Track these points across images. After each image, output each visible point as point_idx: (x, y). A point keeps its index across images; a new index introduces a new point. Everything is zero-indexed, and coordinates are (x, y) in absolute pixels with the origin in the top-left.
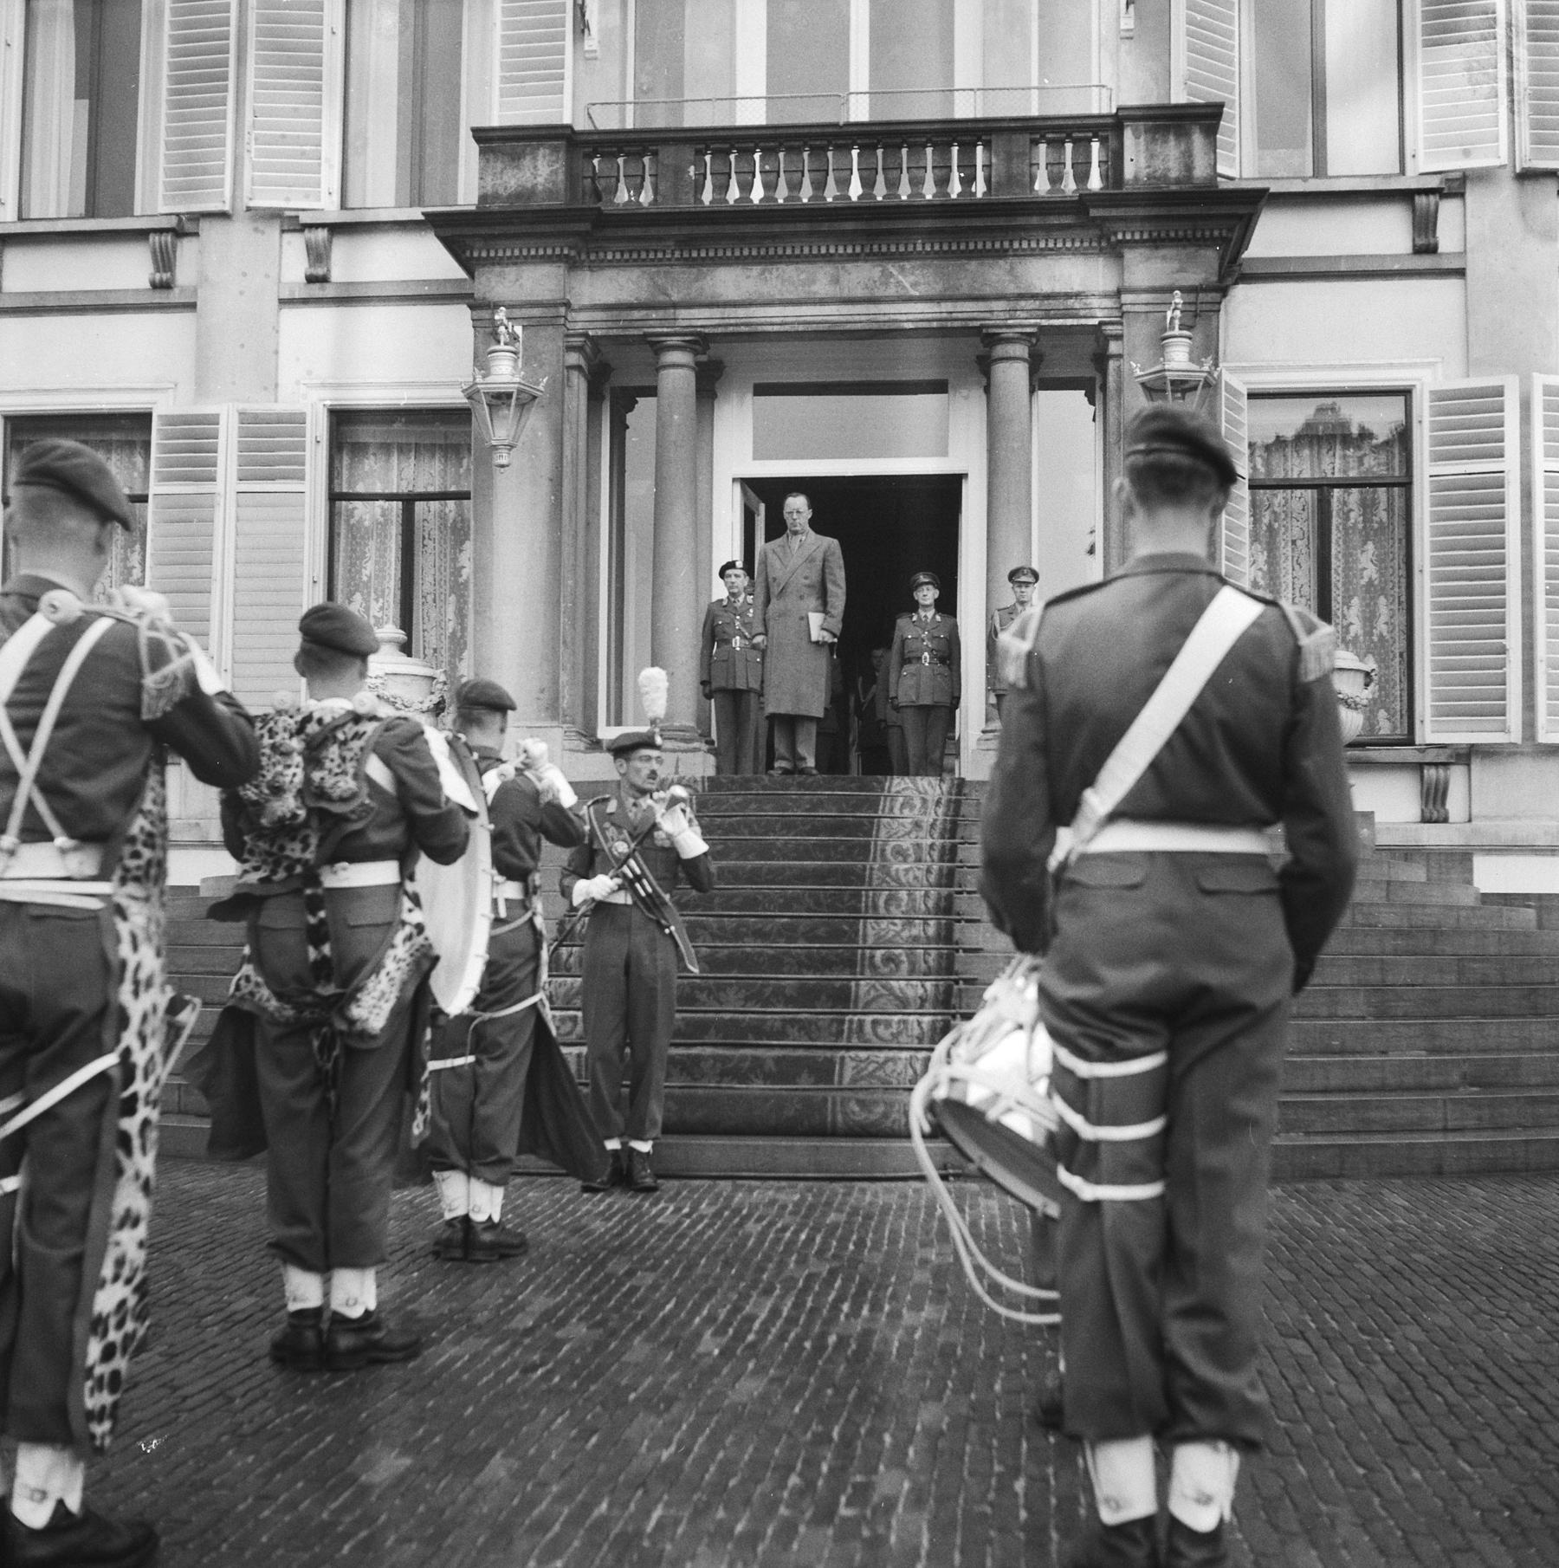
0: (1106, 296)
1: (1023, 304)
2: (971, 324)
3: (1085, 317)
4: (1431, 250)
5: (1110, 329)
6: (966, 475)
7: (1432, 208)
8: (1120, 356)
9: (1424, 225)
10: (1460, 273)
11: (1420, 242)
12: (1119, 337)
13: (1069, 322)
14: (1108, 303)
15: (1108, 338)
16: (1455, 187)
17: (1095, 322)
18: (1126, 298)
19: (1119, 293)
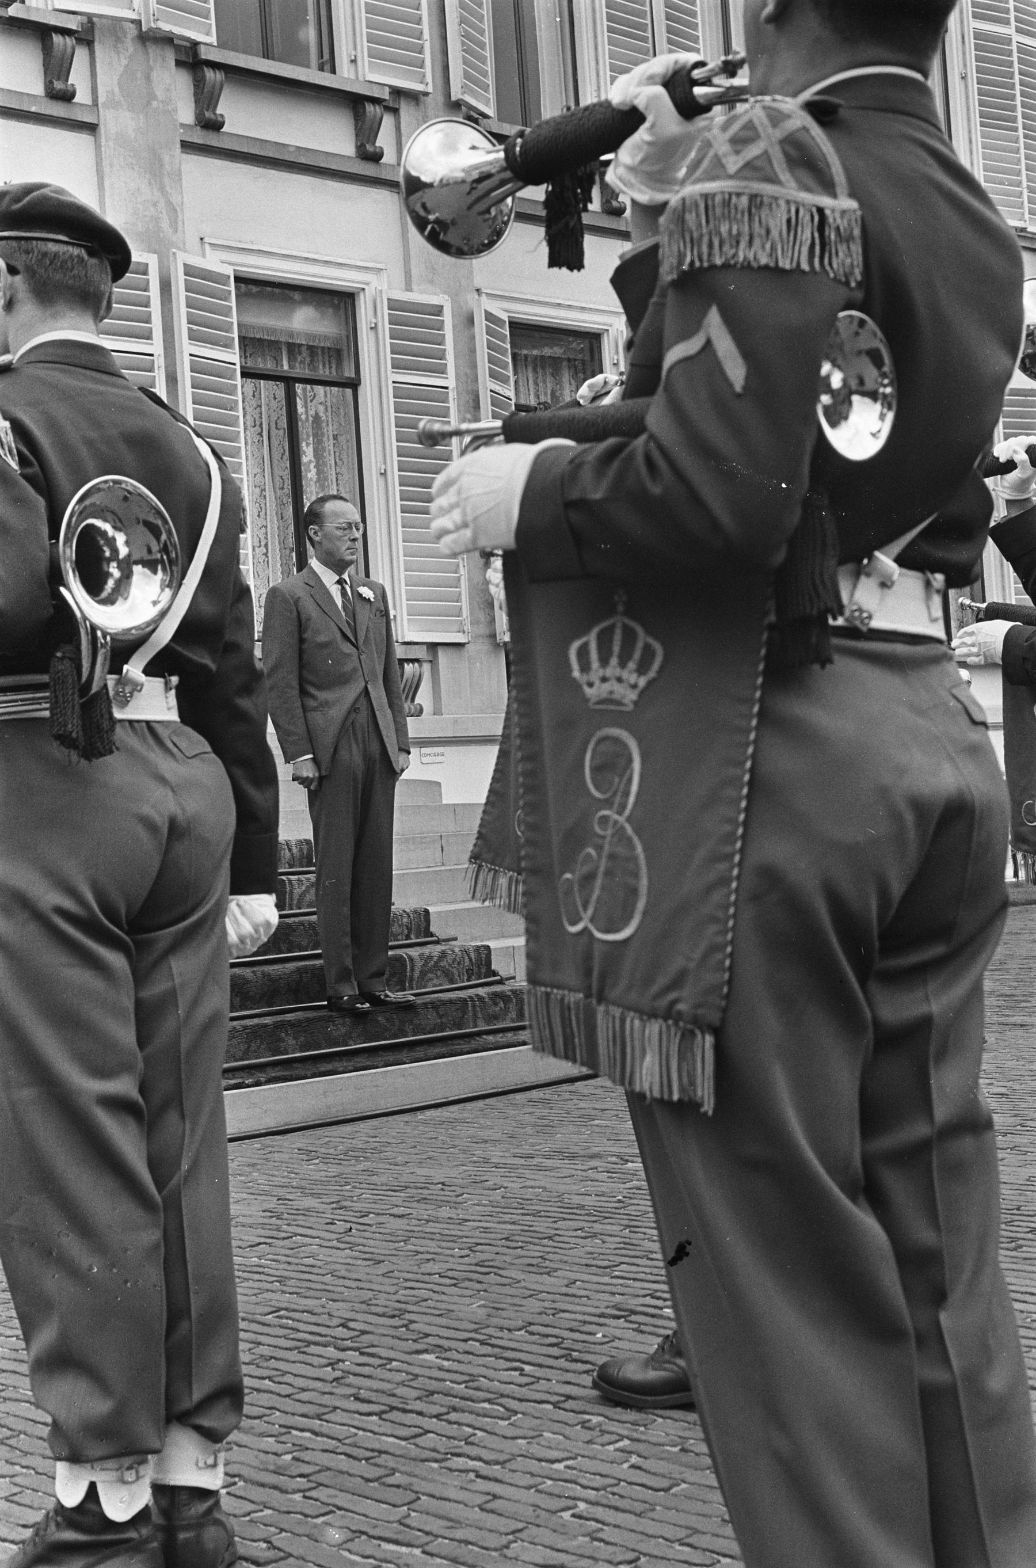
4: (67, 97)
7: (69, 50)
9: (56, 69)
10: (91, 128)
11: (58, 85)
16: (87, 33)
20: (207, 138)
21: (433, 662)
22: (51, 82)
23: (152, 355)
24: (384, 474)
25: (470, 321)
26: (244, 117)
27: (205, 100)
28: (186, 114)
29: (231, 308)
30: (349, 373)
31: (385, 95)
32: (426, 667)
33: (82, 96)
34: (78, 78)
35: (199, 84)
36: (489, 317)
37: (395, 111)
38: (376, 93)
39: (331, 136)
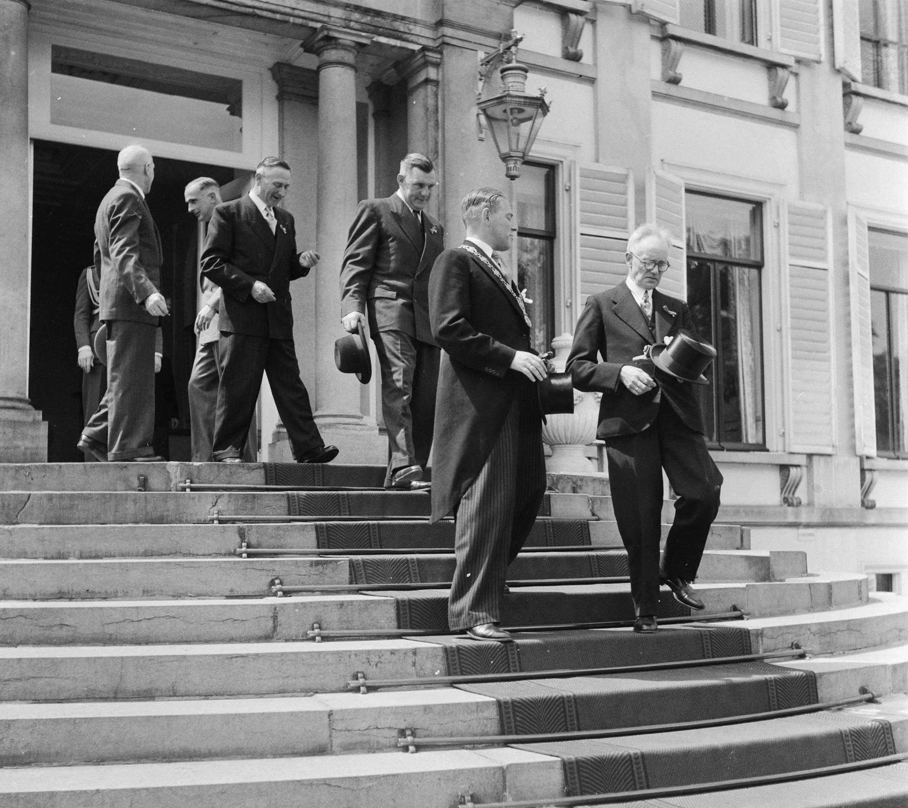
0: (425, 25)
1: (356, 16)
2: (311, 24)
4: (575, 58)
5: (433, 56)
8: (436, 83)
9: (571, 37)
10: (592, 81)
11: (572, 50)
12: (437, 65)
14: (428, 33)
15: (426, 64)
17: (417, 48)
18: (448, 31)
19: (441, 23)
21: (809, 466)
22: (567, 48)
23: (626, 240)
24: (780, 330)
25: (845, 222)
27: (670, 62)
28: (656, 71)
29: (681, 209)
30: (754, 257)
31: (791, 62)
32: (805, 470)
33: (587, 59)
34: (585, 46)
35: (666, 52)
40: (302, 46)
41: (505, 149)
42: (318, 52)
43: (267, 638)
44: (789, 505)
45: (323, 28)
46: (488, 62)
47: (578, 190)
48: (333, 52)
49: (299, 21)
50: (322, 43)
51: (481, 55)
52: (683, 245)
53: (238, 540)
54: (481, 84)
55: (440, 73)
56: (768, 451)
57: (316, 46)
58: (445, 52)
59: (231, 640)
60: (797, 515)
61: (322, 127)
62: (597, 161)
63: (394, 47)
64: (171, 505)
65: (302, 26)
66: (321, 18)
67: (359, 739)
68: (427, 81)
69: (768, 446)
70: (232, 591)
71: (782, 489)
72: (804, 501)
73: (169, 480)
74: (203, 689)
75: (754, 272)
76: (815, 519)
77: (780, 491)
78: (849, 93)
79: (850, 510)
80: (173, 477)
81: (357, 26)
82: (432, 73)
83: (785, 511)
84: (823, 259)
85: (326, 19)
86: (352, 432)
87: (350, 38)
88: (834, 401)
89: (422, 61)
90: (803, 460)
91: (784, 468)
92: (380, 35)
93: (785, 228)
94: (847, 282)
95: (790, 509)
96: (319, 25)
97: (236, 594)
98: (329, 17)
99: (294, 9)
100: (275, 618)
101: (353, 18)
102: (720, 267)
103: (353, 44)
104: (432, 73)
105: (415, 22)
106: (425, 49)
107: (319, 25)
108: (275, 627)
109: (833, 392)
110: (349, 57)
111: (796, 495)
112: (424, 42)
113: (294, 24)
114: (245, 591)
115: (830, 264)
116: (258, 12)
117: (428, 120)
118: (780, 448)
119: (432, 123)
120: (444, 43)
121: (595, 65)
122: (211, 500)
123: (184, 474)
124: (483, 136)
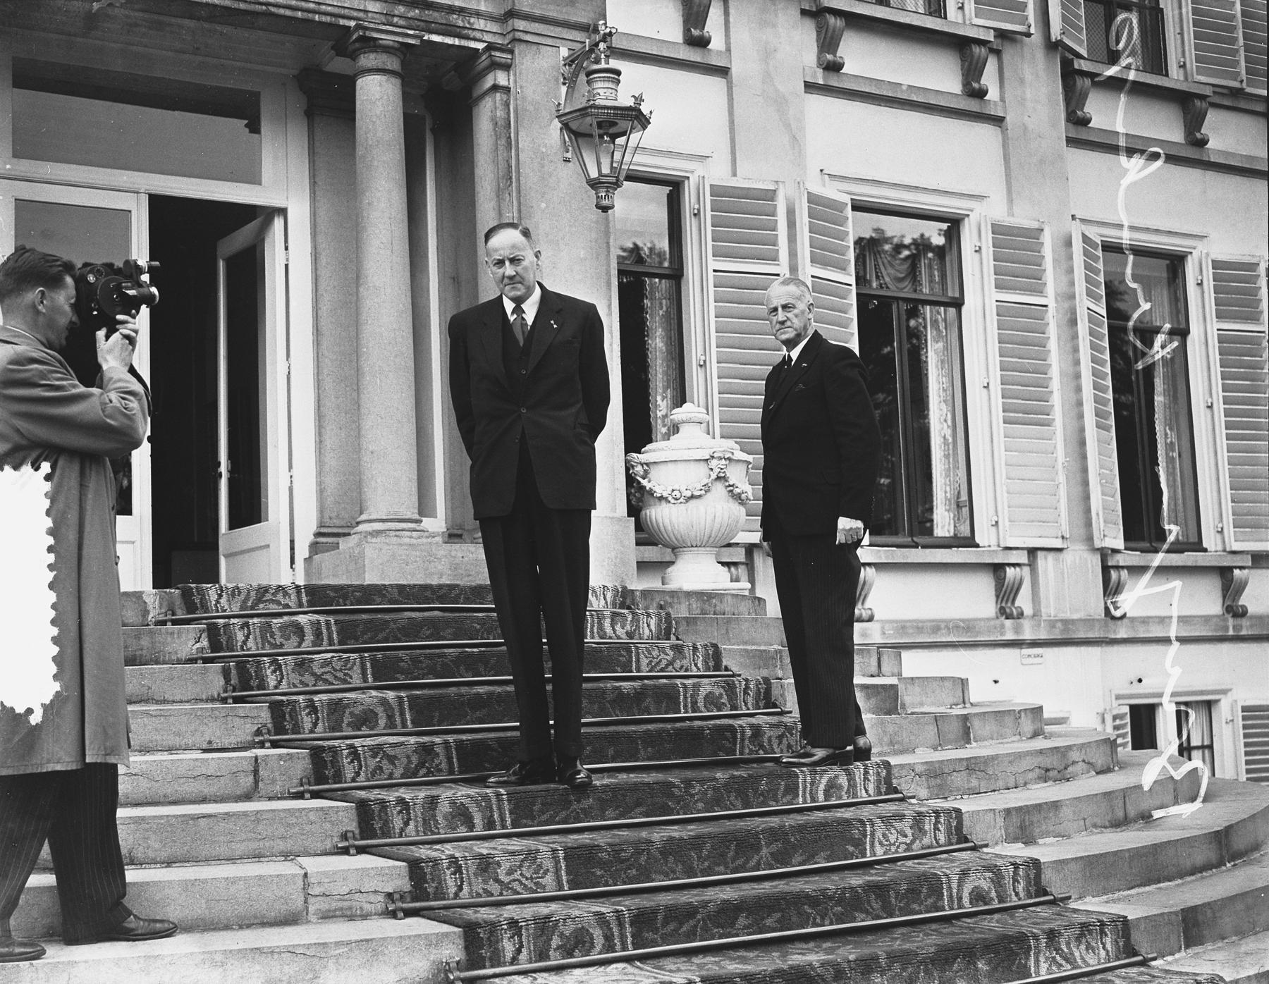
2: (342, 22)
3: (468, 38)
4: (701, 43)
6: (283, 212)
8: (507, 90)
10: (723, 72)
11: (695, 32)
12: (506, 67)
13: (449, 41)
15: (495, 66)
17: (481, 46)
18: (521, 24)
20: (830, 81)
21: (1032, 564)
22: (689, 30)
25: (1069, 243)
26: (863, 58)
27: (828, 43)
30: (952, 293)
31: (990, 36)
32: (1026, 570)
33: (717, 44)
36: (1086, 239)
37: (998, 53)
38: (982, 35)
39: (938, 75)
40: (332, 48)
41: (594, 174)
42: (354, 56)
43: (247, 797)
44: (1007, 618)
45: (358, 27)
46: (573, 61)
47: (709, 213)
48: (372, 56)
49: (327, 19)
50: (357, 45)
51: (564, 52)
52: (852, 280)
53: (222, 682)
54: (564, 89)
55: (512, 78)
56: (977, 546)
57: (351, 48)
58: (517, 52)
59: (204, 800)
60: (1017, 630)
61: (360, 151)
62: (734, 174)
63: (453, 46)
64: (145, 642)
65: (330, 24)
66: (355, 14)
67: (340, 904)
68: (495, 88)
69: (978, 540)
70: (210, 742)
71: (997, 597)
72: (1028, 611)
73: (146, 612)
74: (164, 855)
75: (952, 311)
76: (1043, 635)
77: (994, 599)
78: (1069, 74)
79: (1089, 622)
80: (150, 607)
81: (402, 22)
82: (501, 78)
83: (1003, 626)
84: (1039, 291)
85: (361, 15)
86: (407, 540)
87: (392, 38)
88: (1062, 478)
89: (486, 63)
90: (1022, 558)
91: (997, 569)
92: (431, 32)
93: (988, 251)
94: (1073, 322)
95: (1008, 623)
96: (352, 23)
97: (215, 746)
98: (366, 12)
99: (319, 4)
100: (256, 772)
101: (396, 12)
102: (904, 307)
103: (396, 45)
104: (501, 78)
105: (478, 14)
106: (491, 47)
107: (352, 23)
108: (256, 782)
109: (1060, 467)
110: (393, 63)
111: (1017, 604)
112: (488, 38)
113: (320, 23)
114: (226, 742)
115: (1050, 299)
116: (273, 9)
117: (498, 137)
118: (993, 542)
119: (503, 142)
120: (515, 40)
121: (728, 50)
122: (192, 635)
123: (165, 603)
124: (569, 155)
